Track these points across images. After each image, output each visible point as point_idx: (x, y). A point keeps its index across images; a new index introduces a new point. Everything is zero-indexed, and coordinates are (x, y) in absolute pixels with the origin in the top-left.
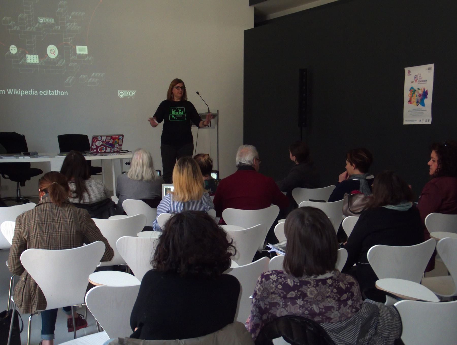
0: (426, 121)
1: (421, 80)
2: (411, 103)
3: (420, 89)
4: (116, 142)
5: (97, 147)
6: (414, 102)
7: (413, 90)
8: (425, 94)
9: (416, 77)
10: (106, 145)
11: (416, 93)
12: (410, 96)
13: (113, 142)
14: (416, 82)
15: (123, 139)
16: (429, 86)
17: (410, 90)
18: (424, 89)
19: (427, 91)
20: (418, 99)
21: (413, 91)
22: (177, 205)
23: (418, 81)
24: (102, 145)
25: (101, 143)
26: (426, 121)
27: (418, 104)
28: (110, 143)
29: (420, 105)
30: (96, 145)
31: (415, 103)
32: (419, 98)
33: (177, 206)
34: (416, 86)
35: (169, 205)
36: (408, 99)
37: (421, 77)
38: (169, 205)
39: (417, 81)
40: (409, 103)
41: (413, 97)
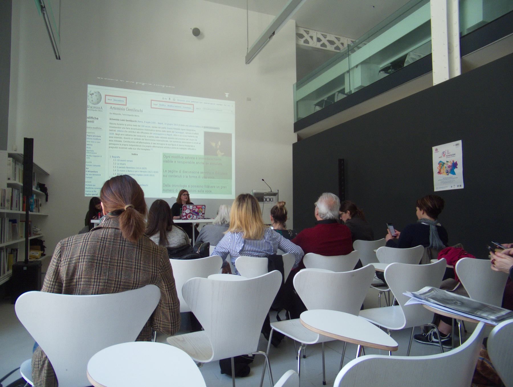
0: (458, 186)
1: (449, 154)
2: (440, 174)
3: (449, 161)
4: (200, 210)
5: (187, 214)
6: (443, 172)
7: (442, 163)
8: (455, 165)
9: (443, 153)
10: (193, 213)
11: (445, 166)
12: (439, 168)
13: (198, 211)
14: (444, 157)
15: (205, 208)
16: (459, 158)
17: (439, 164)
18: (453, 161)
19: (456, 162)
20: (448, 170)
21: (441, 164)
22: (238, 241)
23: (446, 156)
24: (190, 213)
25: (189, 211)
26: (458, 186)
27: (448, 174)
28: (196, 211)
29: (450, 174)
30: (185, 213)
31: (445, 173)
32: (449, 169)
33: (237, 243)
34: (444, 160)
35: (228, 242)
36: (438, 171)
37: (449, 152)
38: (228, 242)
39: (445, 156)
40: (438, 174)
41: (442, 169)
